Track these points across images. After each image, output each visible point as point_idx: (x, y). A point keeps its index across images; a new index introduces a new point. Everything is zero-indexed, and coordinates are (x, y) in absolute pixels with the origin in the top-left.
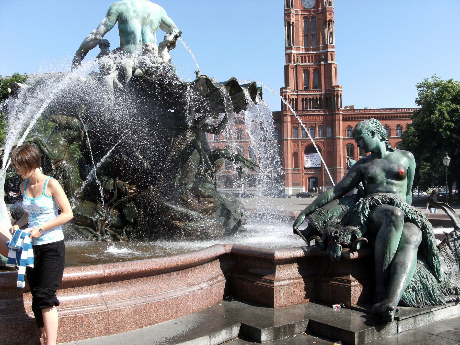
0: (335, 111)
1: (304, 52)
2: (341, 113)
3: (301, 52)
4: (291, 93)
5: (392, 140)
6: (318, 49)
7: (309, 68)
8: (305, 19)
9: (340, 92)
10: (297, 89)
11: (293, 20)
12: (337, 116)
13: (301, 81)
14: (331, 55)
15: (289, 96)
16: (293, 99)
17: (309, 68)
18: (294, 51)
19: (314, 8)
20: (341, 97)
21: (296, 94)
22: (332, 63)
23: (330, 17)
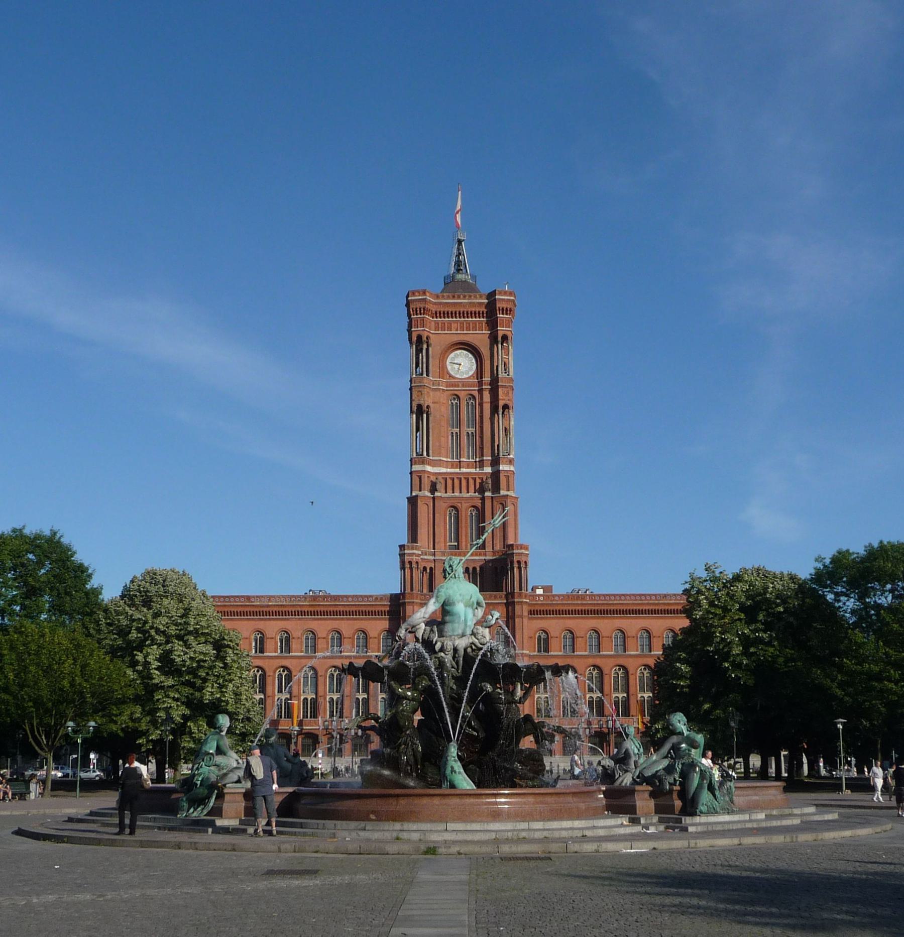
0: (513, 597)
1: (449, 470)
2: (526, 602)
3: (444, 470)
4: (422, 557)
5: (631, 660)
6: (481, 464)
7: (461, 503)
8: (454, 399)
9: (523, 559)
10: (434, 549)
11: (427, 400)
12: (517, 607)
13: (443, 531)
14: (508, 478)
15: (417, 563)
16: (425, 568)
17: (461, 503)
18: (429, 468)
19: (472, 375)
20: (526, 568)
21: (432, 558)
22: (507, 495)
23: (507, 398)
